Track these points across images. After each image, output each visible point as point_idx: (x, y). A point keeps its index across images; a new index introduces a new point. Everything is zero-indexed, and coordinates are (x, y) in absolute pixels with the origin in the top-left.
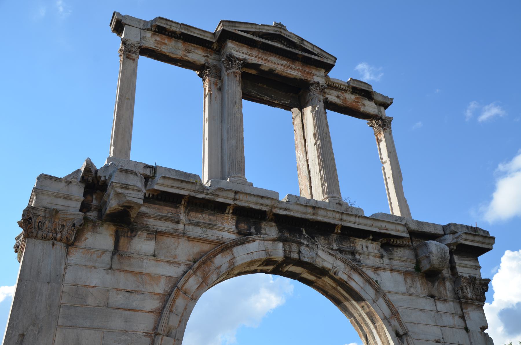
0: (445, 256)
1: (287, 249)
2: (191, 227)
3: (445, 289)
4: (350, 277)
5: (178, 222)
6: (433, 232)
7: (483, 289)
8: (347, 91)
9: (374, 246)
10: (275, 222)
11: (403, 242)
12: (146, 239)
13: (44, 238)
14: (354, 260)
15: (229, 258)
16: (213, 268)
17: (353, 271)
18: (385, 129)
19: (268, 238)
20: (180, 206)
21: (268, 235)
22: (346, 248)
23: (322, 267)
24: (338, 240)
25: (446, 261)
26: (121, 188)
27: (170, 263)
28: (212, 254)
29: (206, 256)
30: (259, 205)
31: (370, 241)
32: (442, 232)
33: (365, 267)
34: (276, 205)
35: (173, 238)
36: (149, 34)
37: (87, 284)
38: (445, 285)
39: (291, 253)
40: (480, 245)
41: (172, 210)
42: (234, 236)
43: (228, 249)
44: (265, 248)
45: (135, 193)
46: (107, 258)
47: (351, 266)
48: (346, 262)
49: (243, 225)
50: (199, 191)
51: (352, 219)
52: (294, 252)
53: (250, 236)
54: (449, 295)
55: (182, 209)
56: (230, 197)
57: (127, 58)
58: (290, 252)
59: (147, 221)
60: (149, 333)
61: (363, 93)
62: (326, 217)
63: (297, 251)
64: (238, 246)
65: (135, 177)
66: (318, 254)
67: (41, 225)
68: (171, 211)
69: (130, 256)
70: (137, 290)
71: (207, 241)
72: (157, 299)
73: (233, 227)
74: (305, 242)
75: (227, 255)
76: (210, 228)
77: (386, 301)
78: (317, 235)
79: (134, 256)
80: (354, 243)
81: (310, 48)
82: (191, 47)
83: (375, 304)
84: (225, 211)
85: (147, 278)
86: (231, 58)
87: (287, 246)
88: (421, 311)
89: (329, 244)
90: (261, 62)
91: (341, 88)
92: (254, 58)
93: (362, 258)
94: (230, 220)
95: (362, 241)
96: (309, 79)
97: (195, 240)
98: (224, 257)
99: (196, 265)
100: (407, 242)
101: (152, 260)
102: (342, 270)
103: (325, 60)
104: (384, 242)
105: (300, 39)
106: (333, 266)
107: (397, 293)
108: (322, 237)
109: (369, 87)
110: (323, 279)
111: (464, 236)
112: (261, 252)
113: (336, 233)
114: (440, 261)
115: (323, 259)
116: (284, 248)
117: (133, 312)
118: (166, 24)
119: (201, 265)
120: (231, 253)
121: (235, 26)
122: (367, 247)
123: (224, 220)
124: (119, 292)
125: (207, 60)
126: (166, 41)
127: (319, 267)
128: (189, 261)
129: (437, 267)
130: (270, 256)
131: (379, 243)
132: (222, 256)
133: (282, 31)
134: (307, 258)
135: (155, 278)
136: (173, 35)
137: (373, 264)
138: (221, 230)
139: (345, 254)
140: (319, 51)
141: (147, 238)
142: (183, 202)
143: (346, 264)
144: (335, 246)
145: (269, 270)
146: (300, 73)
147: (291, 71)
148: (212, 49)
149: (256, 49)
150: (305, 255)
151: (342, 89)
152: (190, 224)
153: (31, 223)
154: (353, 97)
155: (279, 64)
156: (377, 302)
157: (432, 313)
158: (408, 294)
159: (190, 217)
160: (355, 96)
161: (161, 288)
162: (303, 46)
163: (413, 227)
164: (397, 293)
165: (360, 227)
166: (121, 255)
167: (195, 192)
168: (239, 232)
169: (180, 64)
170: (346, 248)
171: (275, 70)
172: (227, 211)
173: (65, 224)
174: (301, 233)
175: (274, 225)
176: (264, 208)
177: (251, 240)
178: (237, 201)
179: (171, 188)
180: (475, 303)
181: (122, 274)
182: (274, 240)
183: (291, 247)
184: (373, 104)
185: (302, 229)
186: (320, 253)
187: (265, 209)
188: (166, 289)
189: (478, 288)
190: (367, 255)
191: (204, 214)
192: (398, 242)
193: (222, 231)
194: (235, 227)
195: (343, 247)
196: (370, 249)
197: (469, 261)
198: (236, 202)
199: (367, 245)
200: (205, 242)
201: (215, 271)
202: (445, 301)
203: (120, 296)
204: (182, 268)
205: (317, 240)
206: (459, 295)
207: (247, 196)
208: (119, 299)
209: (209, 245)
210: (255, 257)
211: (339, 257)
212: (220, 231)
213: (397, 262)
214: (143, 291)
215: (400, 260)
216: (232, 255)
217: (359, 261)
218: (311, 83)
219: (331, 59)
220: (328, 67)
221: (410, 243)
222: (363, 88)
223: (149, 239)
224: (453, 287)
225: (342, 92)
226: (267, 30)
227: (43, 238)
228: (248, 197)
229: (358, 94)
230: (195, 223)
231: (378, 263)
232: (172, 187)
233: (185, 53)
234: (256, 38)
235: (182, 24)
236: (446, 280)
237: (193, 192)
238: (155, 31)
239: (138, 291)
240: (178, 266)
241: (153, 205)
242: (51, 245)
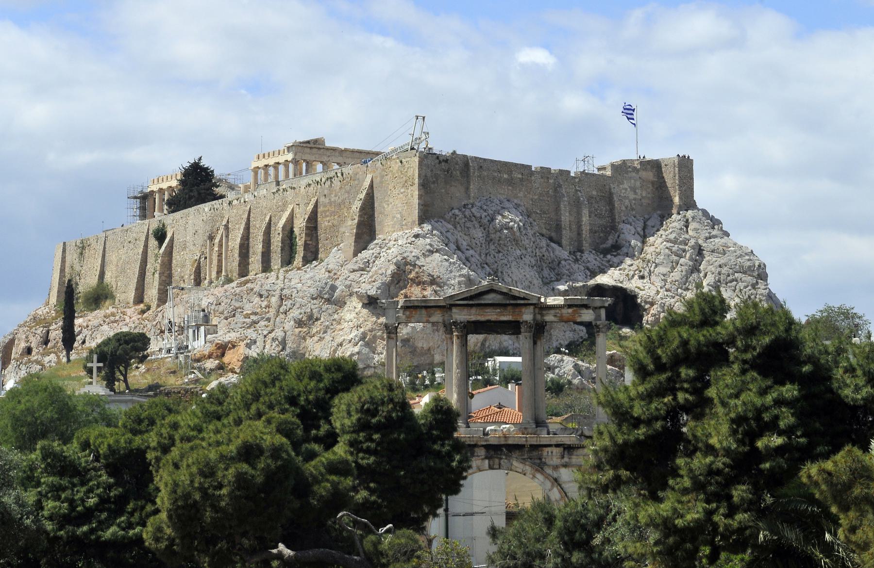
8: (564, 307)
58: (493, 465)
74: (504, 457)
77: (558, 489)
82: (432, 311)
96: (518, 320)
103: (530, 302)
107: (569, 482)
108: (518, 451)
122: (552, 453)
146: (511, 317)
151: (559, 307)
154: (570, 311)
164: (569, 482)
174: (502, 450)
176: (472, 443)
184: (591, 311)
186: (515, 463)
196: (554, 453)
217: (545, 463)
234: (471, 302)
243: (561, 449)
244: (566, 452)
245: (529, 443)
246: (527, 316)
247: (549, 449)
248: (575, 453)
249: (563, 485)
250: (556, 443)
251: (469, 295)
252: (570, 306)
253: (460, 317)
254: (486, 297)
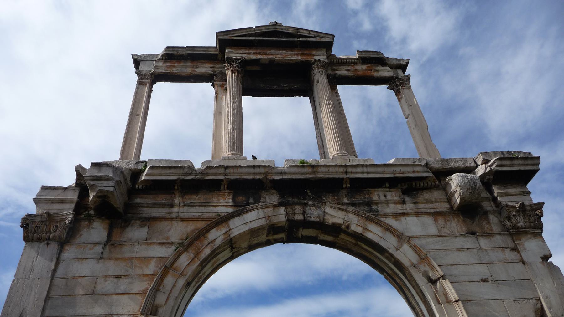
0: (476, 186)
1: (289, 213)
2: (186, 209)
3: (489, 223)
4: (365, 229)
5: (172, 206)
6: (462, 167)
7: (537, 215)
10: (275, 189)
11: (427, 183)
12: (139, 227)
13: (39, 240)
14: (371, 210)
15: (224, 231)
16: (206, 243)
17: (368, 222)
19: (267, 205)
20: (174, 192)
21: (268, 202)
22: (358, 201)
23: (332, 224)
24: (350, 194)
25: (478, 191)
26: (93, 180)
27: (161, 244)
28: (205, 230)
29: (198, 232)
30: (252, 175)
31: (388, 189)
33: (383, 216)
34: (270, 172)
35: (166, 222)
36: (160, 63)
37: (77, 275)
38: (488, 219)
39: (294, 215)
40: (522, 168)
41: (167, 197)
42: (230, 210)
43: (223, 223)
44: (265, 215)
45: (106, 182)
46: (99, 249)
47: (365, 217)
48: (359, 214)
49: (241, 198)
50: (188, 174)
51: (359, 170)
52: (298, 214)
53: (247, 207)
54: (496, 228)
55: (177, 194)
56: (220, 173)
57: (140, 84)
58: (294, 214)
59: (141, 211)
60: (135, 314)
61: (374, 61)
62: (328, 173)
63: (301, 212)
64: (234, 217)
65: (108, 168)
66: (326, 211)
67: (37, 229)
68: (165, 198)
69: (121, 244)
70: (126, 274)
71: (202, 218)
72: (146, 281)
73: (230, 201)
74: (310, 202)
75: (222, 228)
76: (205, 206)
77: (411, 247)
78: (324, 194)
79: (126, 244)
80: (369, 194)
81: (306, 33)
83: (398, 251)
84: (221, 189)
85: (137, 262)
87: (290, 210)
88: (459, 251)
89: (338, 199)
90: (259, 57)
91: (350, 62)
92: (252, 55)
93: (380, 208)
94: (227, 195)
95: (378, 190)
96: (309, 59)
97: (188, 220)
98: (219, 230)
99: (186, 242)
100: (432, 183)
101: (144, 244)
102: (356, 222)
104: (404, 187)
105: (295, 29)
106: (344, 221)
108: (330, 195)
109: (379, 54)
110: (340, 237)
111: (499, 162)
112: (260, 219)
113: (346, 188)
114: (471, 192)
115: (332, 215)
116: (286, 212)
117: (120, 297)
118: (173, 51)
119: (192, 242)
120: (226, 226)
122: (385, 196)
123: (221, 196)
124: (108, 279)
126: (176, 64)
127: (329, 224)
128: (181, 240)
129: (469, 200)
130: (270, 221)
131: (399, 189)
132: (217, 230)
133: (277, 27)
134: (314, 217)
135: (145, 261)
136: (182, 58)
137: (394, 212)
138: (217, 206)
139: (358, 207)
140: (315, 34)
141: (140, 225)
142: (176, 188)
143: (360, 216)
144: (346, 201)
145: (284, 239)
146: (300, 57)
147: (291, 57)
148: (218, 60)
149: (254, 48)
150: (311, 215)
151: (352, 63)
152: (184, 206)
153: (27, 229)
154: (364, 67)
155: (278, 55)
156: (401, 250)
157: (475, 250)
159: (185, 200)
160: (367, 66)
161: (151, 269)
162: (299, 33)
163: (437, 165)
165: (370, 176)
166: (113, 245)
167: (184, 175)
168: (236, 205)
169: (193, 80)
170: (358, 201)
171: (275, 61)
172: (222, 188)
173: (58, 225)
175: (275, 192)
176: (258, 177)
177: (249, 210)
178: (228, 175)
179: (160, 175)
180: (530, 231)
181: (112, 262)
182: (275, 206)
183: (294, 209)
184: (388, 68)
185: (306, 190)
186: (329, 210)
187: (259, 178)
188: (156, 269)
189: (530, 215)
190: (386, 204)
191: (200, 194)
192: (422, 184)
193: (218, 207)
194: (232, 201)
195: (356, 200)
196: (389, 197)
197: (514, 188)
198: (227, 177)
199: (385, 194)
200: (200, 220)
201: (209, 245)
202: (489, 235)
203: (109, 282)
204: (173, 248)
205: (324, 199)
206: (507, 226)
207: (238, 169)
208: (109, 286)
209: (203, 222)
210: (254, 225)
211: (350, 211)
212: (216, 207)
213: (424, 204)
214: (132, 275)
215: (427, 202)
216: (227, 227)
217: (378, 211)
218: (312, 62)
219: (328, 37)
220: (328, 46)
221: (437, 183)
222: (371, 56)
223: (142, 226)
224: (499, 220)
225: (352, 66)
226: (263, 30)
227: (38, 240)
228: (239, 169)
229: (370, 63)
230: (189, 204)
231: (399, 209)
232: (161, 175)
233: (193, 69)
234: (251, 39)
235: (187, 47)
236: (489, 213)
237: (182, 175)
238: (166, 59)
239: (127, 275)
240: (170, 246)
241: (148, 196)
242: (46, 246)
245: (350, 176)
247: (380, 192)
249: (417, 242)
253: (237, 55)
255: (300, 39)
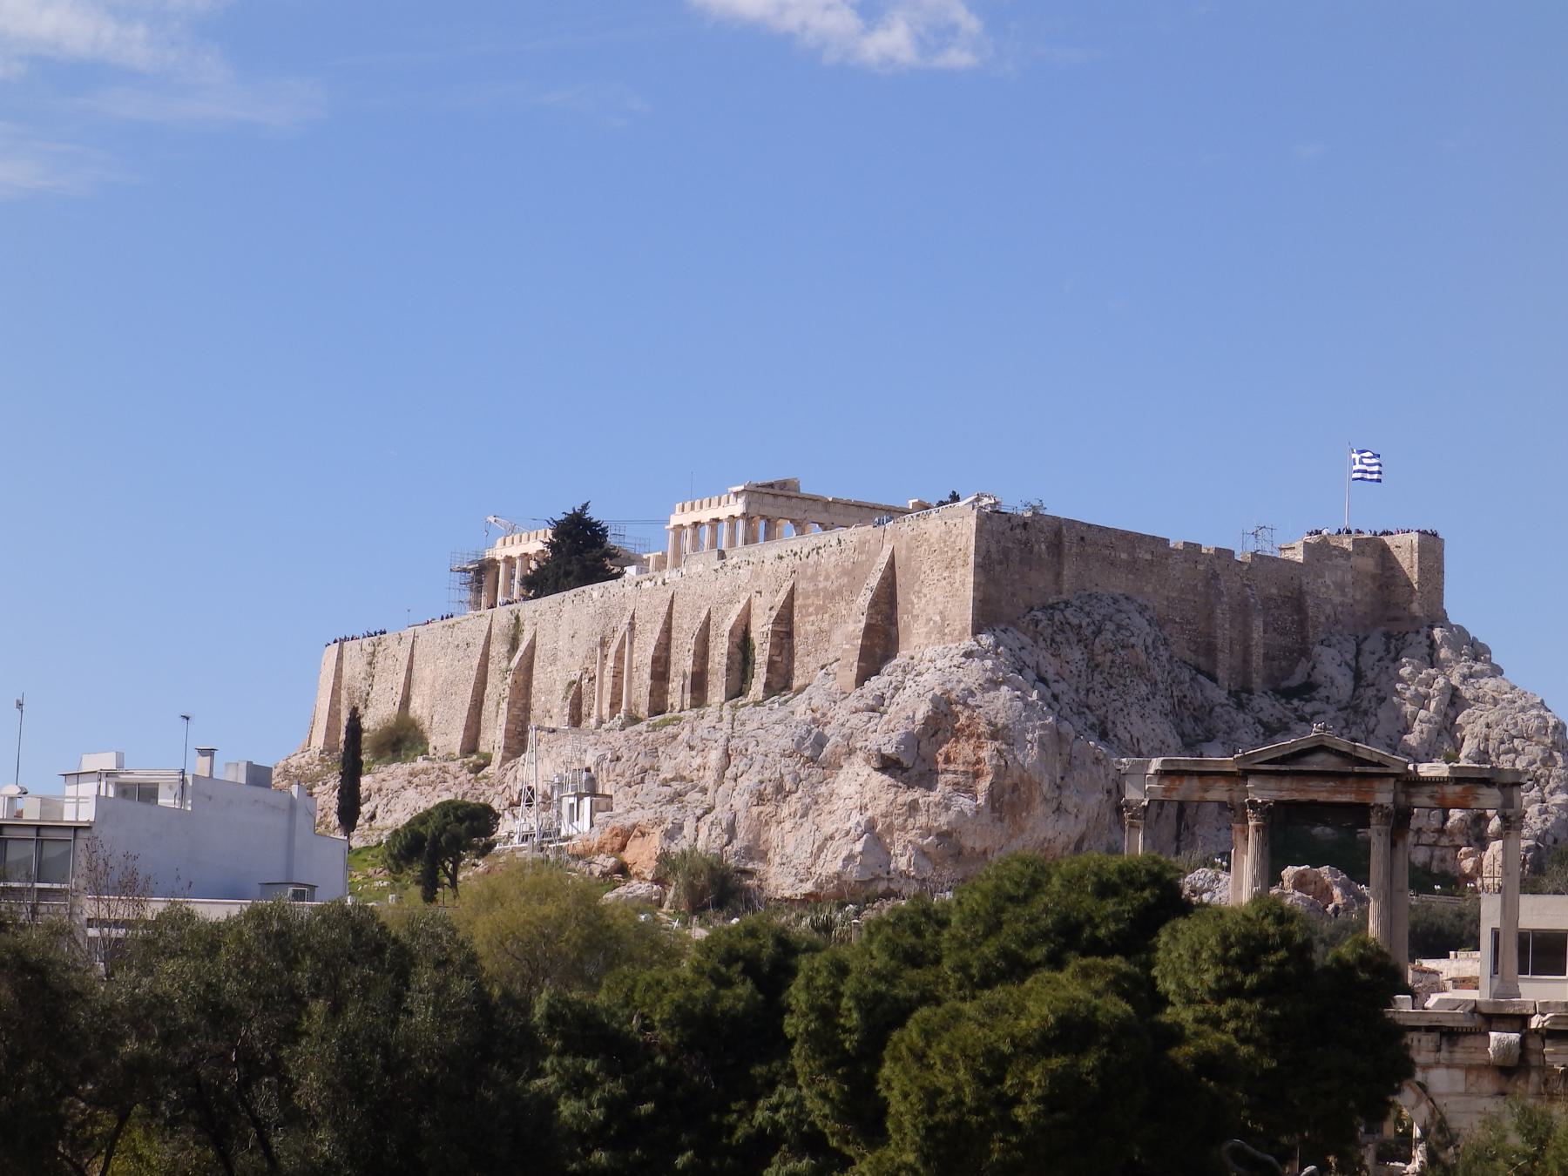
3: (1527, 1082)
9: (1430, 1038)
18: (1508, 833)
32: (1531, 1011)
82: (1210, 781)
86: (1253, 804)
90: (1296, 796)
96: (1367, 801)
103: (1389, 771)
118: (1173, 765)
121: (1254, 759)
122: (1419, 1041)
125: (1230, 798)
146: (1353, 796)
151: (1439, 782)
154: (1458, 789)
158: (1467, 1093)
164: (1448, 1095)
184: (1495, 792)
234: (1284, 768)
243: (1435, 1036)
244: (1444, 1041)
246: (1383, 796)
248: (1461, 1044)
249: (1437, 1101)
250: (1427, 1024)
251: (1280, 754)
252: (1458, 781)
254: (1308, 759)
255: (1357, 769)
